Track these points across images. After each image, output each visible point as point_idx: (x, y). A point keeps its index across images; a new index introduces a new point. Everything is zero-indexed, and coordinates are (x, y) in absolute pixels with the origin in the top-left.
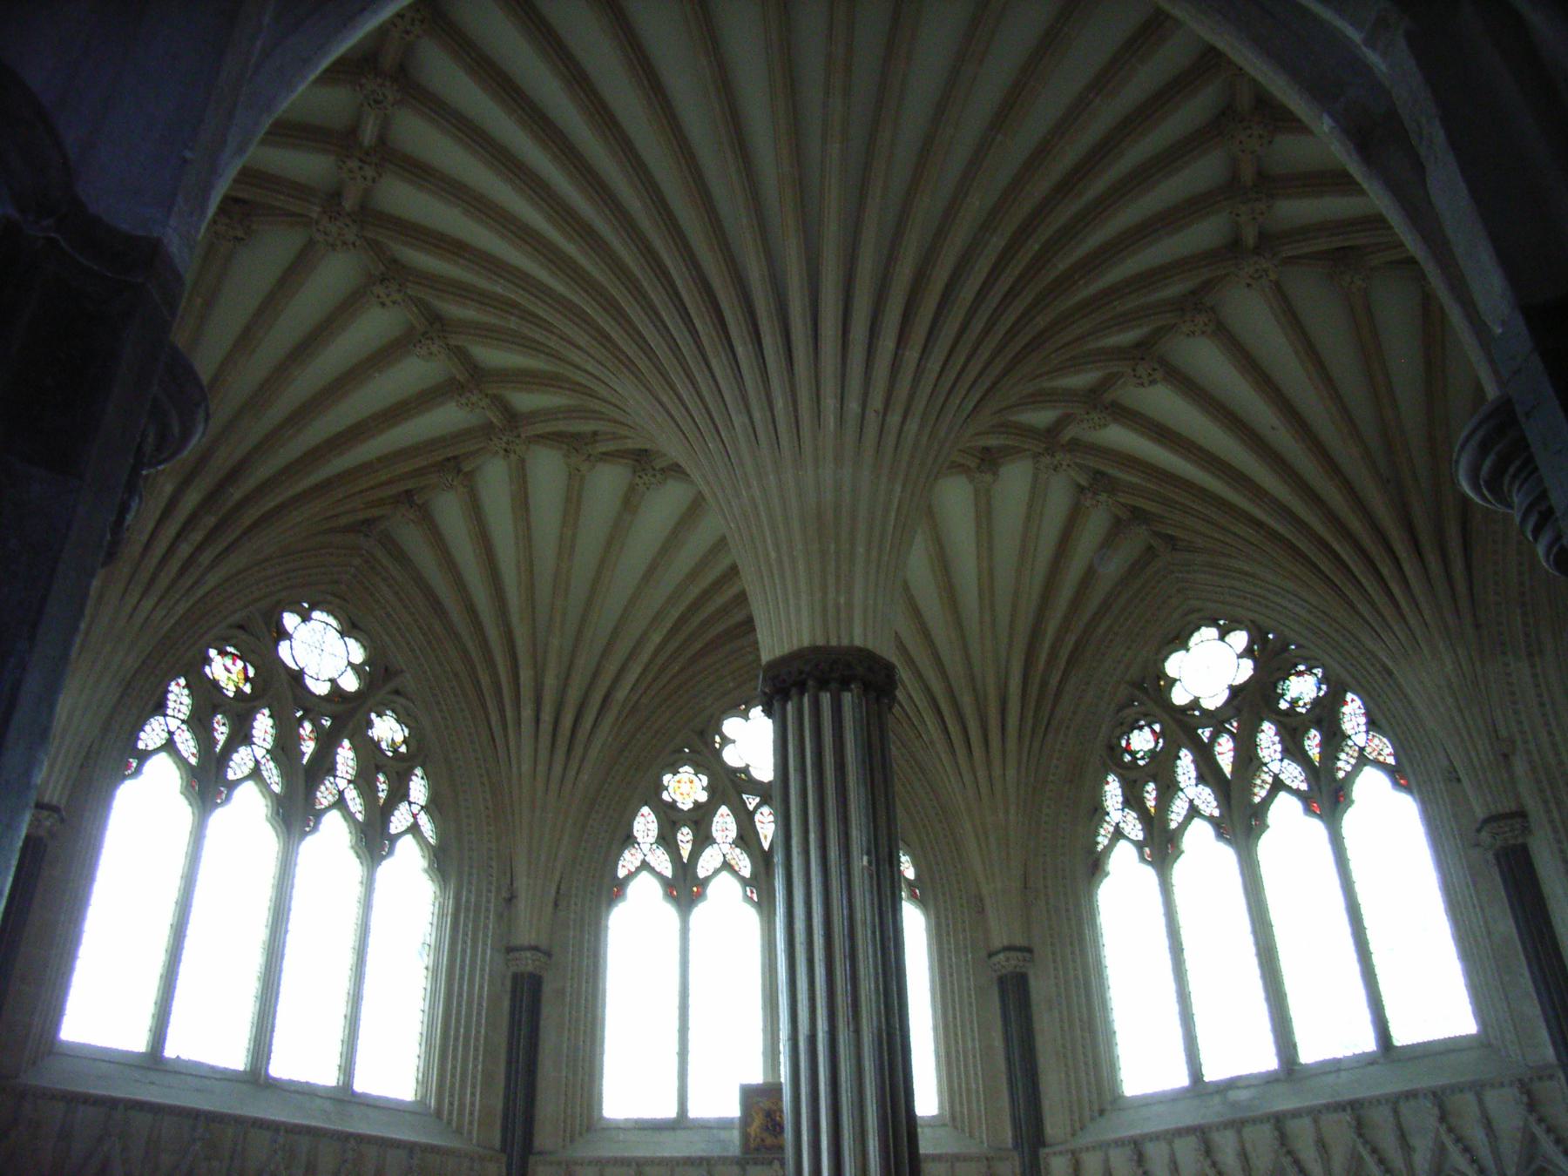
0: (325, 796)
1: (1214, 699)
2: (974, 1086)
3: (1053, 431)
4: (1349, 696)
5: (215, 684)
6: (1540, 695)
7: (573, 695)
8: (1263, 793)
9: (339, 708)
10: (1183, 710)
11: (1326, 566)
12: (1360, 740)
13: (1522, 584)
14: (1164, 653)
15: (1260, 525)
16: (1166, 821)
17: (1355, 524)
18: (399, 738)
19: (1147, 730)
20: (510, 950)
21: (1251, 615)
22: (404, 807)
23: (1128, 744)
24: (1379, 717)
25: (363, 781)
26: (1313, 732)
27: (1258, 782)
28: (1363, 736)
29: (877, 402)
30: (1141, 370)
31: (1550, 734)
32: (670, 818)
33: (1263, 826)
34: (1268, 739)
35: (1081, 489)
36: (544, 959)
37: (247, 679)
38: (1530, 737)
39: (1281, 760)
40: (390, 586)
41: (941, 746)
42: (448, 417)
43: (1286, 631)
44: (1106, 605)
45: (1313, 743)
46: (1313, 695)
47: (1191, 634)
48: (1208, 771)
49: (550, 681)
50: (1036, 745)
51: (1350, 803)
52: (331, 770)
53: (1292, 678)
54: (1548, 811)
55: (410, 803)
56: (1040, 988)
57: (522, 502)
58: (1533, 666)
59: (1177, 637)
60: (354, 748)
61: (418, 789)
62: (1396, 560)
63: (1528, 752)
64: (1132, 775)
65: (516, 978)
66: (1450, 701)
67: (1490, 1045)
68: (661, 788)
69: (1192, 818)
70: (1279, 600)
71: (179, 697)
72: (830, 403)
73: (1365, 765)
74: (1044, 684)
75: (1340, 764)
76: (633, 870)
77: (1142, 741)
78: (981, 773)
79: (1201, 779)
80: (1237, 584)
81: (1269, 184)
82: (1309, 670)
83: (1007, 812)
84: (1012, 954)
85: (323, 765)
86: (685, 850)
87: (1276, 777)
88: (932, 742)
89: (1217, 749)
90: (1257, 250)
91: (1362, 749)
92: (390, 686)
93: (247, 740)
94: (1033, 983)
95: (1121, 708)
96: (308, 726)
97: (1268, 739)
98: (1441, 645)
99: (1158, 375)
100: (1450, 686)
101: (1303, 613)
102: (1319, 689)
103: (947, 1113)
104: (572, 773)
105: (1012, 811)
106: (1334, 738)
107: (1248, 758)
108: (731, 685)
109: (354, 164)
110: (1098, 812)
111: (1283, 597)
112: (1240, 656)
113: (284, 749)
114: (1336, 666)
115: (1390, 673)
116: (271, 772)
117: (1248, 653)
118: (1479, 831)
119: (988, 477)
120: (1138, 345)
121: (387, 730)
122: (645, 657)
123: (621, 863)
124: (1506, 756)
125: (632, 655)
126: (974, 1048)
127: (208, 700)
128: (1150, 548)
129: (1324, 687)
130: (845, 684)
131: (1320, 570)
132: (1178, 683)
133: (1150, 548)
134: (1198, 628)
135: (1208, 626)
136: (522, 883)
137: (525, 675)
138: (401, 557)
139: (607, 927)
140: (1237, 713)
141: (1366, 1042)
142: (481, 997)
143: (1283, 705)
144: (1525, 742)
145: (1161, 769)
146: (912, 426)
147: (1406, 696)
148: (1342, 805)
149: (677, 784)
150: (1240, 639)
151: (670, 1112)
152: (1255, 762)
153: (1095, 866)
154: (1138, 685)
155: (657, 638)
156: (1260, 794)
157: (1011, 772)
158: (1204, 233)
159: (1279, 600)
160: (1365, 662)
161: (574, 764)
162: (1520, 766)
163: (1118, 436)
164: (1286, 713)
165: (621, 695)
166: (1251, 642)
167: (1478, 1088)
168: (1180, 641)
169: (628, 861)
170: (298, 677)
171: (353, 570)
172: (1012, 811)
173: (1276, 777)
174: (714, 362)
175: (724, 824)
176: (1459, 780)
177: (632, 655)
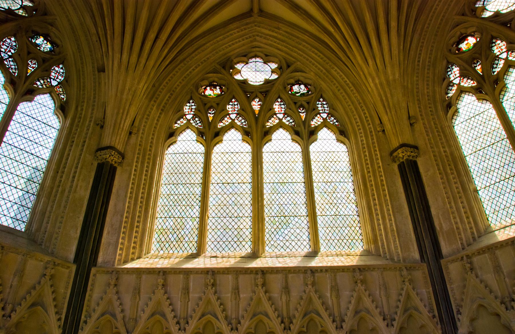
62: (157, 38)
75: (38, 83)
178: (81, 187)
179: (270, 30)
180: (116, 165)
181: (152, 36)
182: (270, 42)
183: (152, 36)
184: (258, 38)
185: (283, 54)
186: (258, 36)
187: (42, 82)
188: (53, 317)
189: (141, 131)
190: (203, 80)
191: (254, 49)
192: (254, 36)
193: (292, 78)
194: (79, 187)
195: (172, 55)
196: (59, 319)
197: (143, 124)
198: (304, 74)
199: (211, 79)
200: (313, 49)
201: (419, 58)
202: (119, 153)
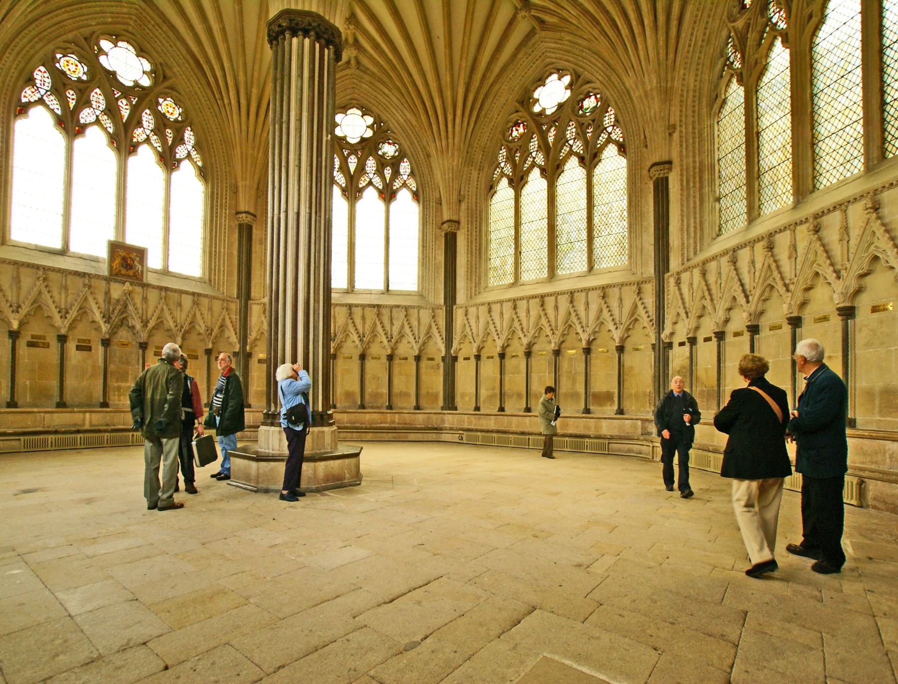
1: (353, 139)
2: (222, 268)
4: (405, 160)
8: (364, 184)
15: (410, 75)
17: (448, 94)
21: (379, 112)
26: (388, 168)
27: (363, 179)
31: (476, 199)
33: (360, 197)
34: (371, 164)
43: (391, 125)
45: (388, 172)
46: (392, 154)
47: (350, 109)
54: (468, 224)
58: (479, 174)
62: (455, 115)
66: (451, 175)
67: (422, 296)
68: (55, 60)
70: (393, 110)
75: (396, 184)
76: (32, 100)
78: (251, 129)
80: (379, 96)
82: (394, 144)
84: (249, 216)
86: (72, 104)
89: (349, 160)
91: (405, 181)
94: (254, 231)
97: (371, 164)
98: (456, 154)
100: (453, 169)
101: (402, 121)
106: (396, 173)
107: (361, 169)
108: (110, 20)
111: (396, 110)
112: (367, 127)
114: (406, 146)
115: (428, 156)
117: (371, 127)
123: (23, 94)
124: (460, 201)
126: (224, 252)
129: (397, 153)
132: (339, 127)
140: (363, 149)
141: (381, 287)
143: (380, 153)
149: (66, 63)
150: (370, 120)
151: (58, 245)
152: (364, 172)
156: (362, 184)
159: (393, 110)
162: (464, 206)
166: (375, 123)
167: (419, 308)
173: (371, 179)
175: (97, 97)
176: (441, 204)
179: (555, 43)
181: (450, 117)
182: (558, 56)
184: (548, 54)
185: (572, 65)
186: (547, 52)
187: (397, 181)
189: (466, 197)
190: (508, 122)
191: (547, 68)
192: (543, 54)
193: (581, 94)
195: (473, 118)
197: (467, 189)
198: (592, 85)
199: (515, 119)
202: (455, 222)
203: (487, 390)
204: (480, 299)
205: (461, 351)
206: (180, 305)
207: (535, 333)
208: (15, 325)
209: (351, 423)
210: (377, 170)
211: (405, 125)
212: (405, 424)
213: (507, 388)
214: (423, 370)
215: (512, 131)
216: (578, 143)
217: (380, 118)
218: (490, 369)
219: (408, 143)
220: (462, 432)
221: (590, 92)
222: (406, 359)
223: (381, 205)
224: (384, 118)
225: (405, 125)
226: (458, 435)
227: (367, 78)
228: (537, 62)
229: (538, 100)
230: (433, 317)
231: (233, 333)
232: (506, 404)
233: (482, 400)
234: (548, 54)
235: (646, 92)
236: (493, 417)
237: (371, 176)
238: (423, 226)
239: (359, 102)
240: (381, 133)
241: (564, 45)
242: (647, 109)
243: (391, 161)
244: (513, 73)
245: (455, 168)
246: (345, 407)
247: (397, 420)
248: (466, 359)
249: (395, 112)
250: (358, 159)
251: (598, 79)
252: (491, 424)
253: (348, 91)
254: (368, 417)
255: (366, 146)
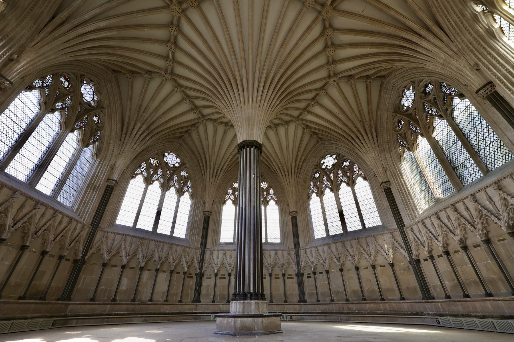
0: (171, 184)
3: (298, 117)
4: (355, 165)
5: (151, 163)
6: (392, 159)
7: (216, 167)
9: (175, 169)
10: (325, 169)
11: (349, 138)
12: (357, 172)
13: (388, 139)
14: (321, 159)
15: (336, 132)
16: (322, 189)
17: (354, 130)
18: (186, 175)
19: (318, 173)
20: (204, 212)
22: (186, 187)
23: (315, 176)
24: (361, 168)
25: (179, 181)
28: (358, 171)
29: (259, 98)
30: (313, 103)
32: (234, 190)
35: (304, 128)
36: (210, 213)
37: (157, 163)
38: (390, 167)
39: (342, 177)
40: (185, 149)
41: (281, 176)
42: (191, 116)
44: (310, 152)
45: (348, 173)
47: (326, 156)
48: (329, 179)
49: (212, 165)
50: (298, 176)
51: (356, 183)
52: (173, 180)
53: (344, 162)
55: (187, 186)
56: (299, 219)
57: (206, 132)
58: (390, 154)
59: (323, 157)
60: (177, 176)
61: (189, 184)
62: (363, 136)
63: (390, 170)
64: (315, 181)
65: (205, 216)
68: (232, 185)
69: (326, 188)
71: (144, 165)
72: (250, 98)
73: (358, 176)
74: (299, 165)
75: (354, 177)
77: (317, 175)
78: (288, 180)
79: (328, 181)
80: (334, 146)
81: (335, 62)
82: (348, 161)
83: (292, 187)
84: (293, 213)
85: (171, 179)
87: (341, 180)
88: (279, 176)
90: (333, 76)
91: (358, 174)
92: (184, 166)
93: (157, 173)
95: (313, 170)
96: (169, 172)
99: (316, 104)
101: (346, 150)
102: (349, 164)
103: (282, 242)
104: (216, 181)
105: (293, 187)
107: (336, 176)
109: (168, 62)
110: (309, 187)
113: (163, 175)
116: (161, 179)
117: (336, 158)
118: (380, 185)
119: (287, 126)
120: (313, 99)
121: (184, 173)
122: (229, 161)
124: (385, 171)
125: (227, 161)
127: (149, 166)
128: (318, 141)
130: (252, 146)
131: (348, 139)
133: (318, 141)
134: (327, 155)
135: (329, 155)
136: (207, 200)
137: (208, 163)
138: (187, 144)
139: (222, 208)
142: (198, 220)
143: (343, 167)
144: (389, 168)
145: (320, 180)
146: (266, 104)
147: (366, 162)
148: (354, 184)
150: (334, 156)
152: (338, 177)
153: (309, 198)
154: (317, 165)
155: (231, 157)
157: (293, 180)
158: (323, 74)
160: (358, 157)
161: (217, 179)
163: (310, 117)
164: (343, 168)
165: (225, 167)
168: (324, 157)
169: (227, 197)
170: (167, 163)
171: (178, 146)
172: (293, 187)
174: (230, 93)
176: (376, 177)
177: (227, 161)
178: (384, 202)
180: (389, 187)
183: (361, 138)
184: (396, 85)
187: (354, 175)
188: (402, 250)
189: (388, 167)
190: (394, 123)
191: (400, 90)
192: (393, 86)
194: (384, 202)
196: (404, 250)
198: (424, 81)
200: (413, 70)
201: (451, 24)
202: (386, 182)
203: (449, 281)
204: (416, 220)
205: (420, 256)
206: (270, 255)
207: (461, 232)
208: (216, 271)
209: (357, 310)
210: (343, 175)
211: (348, 151)
212: (395, 311)
213: (463, 278)
214: (398, 272)
215: (399, 126)
216: (434, 110)
217: (338, 154)
218: (443, 264)
219: (353, 157)
220: (436, 317)
221: (426, 84)
222: (384, 266)
223: (349, 189)
224: (339, 152)
225: (348, 151)
226: (435, 320)
227: (327, 142)
228: (393, 92)
229: (404, 105)
230: (393, 237)
231: (293, 264)
232: (468, 291)
233: (449, 290)
234: (396, 85)
235: (442, 64)
236: (459, 303)
237: (341, 178)
238: (373, 191)
239: (328, 152)
240: (340, 159)
241: (399, 76)
242: (450, 70)
243: (348, 168)
244: (383, 103)
245: (375, 157)
246: (354, 301)
247: (388, 308)
248: (426, 260)
249: (342, 148)
250: (333, 173)
251: (424, 76)
252: (459, 308)
253: (322, 150)
254: (368, 306)
255: (335, 167)
